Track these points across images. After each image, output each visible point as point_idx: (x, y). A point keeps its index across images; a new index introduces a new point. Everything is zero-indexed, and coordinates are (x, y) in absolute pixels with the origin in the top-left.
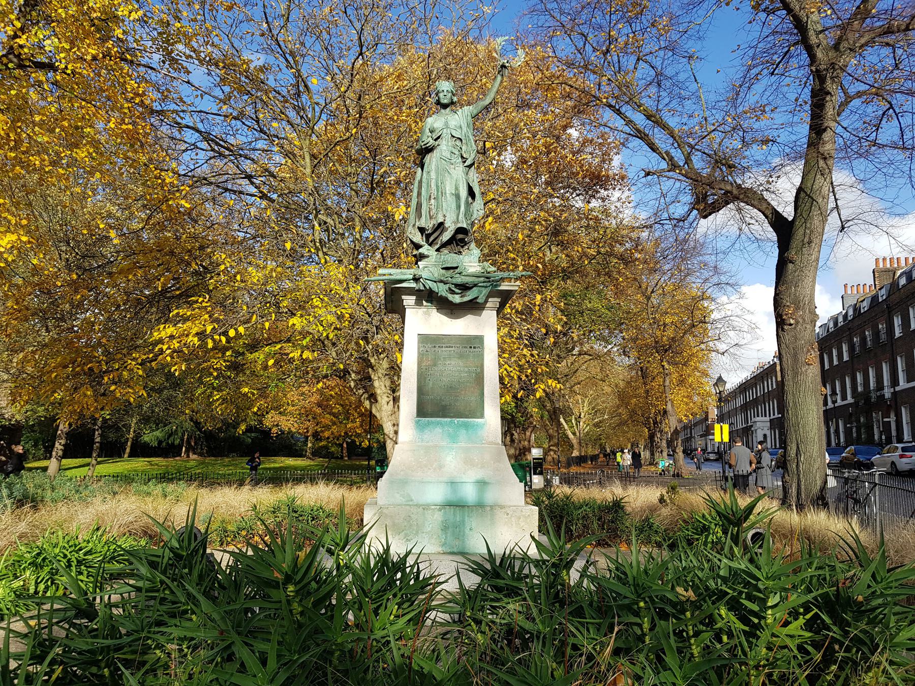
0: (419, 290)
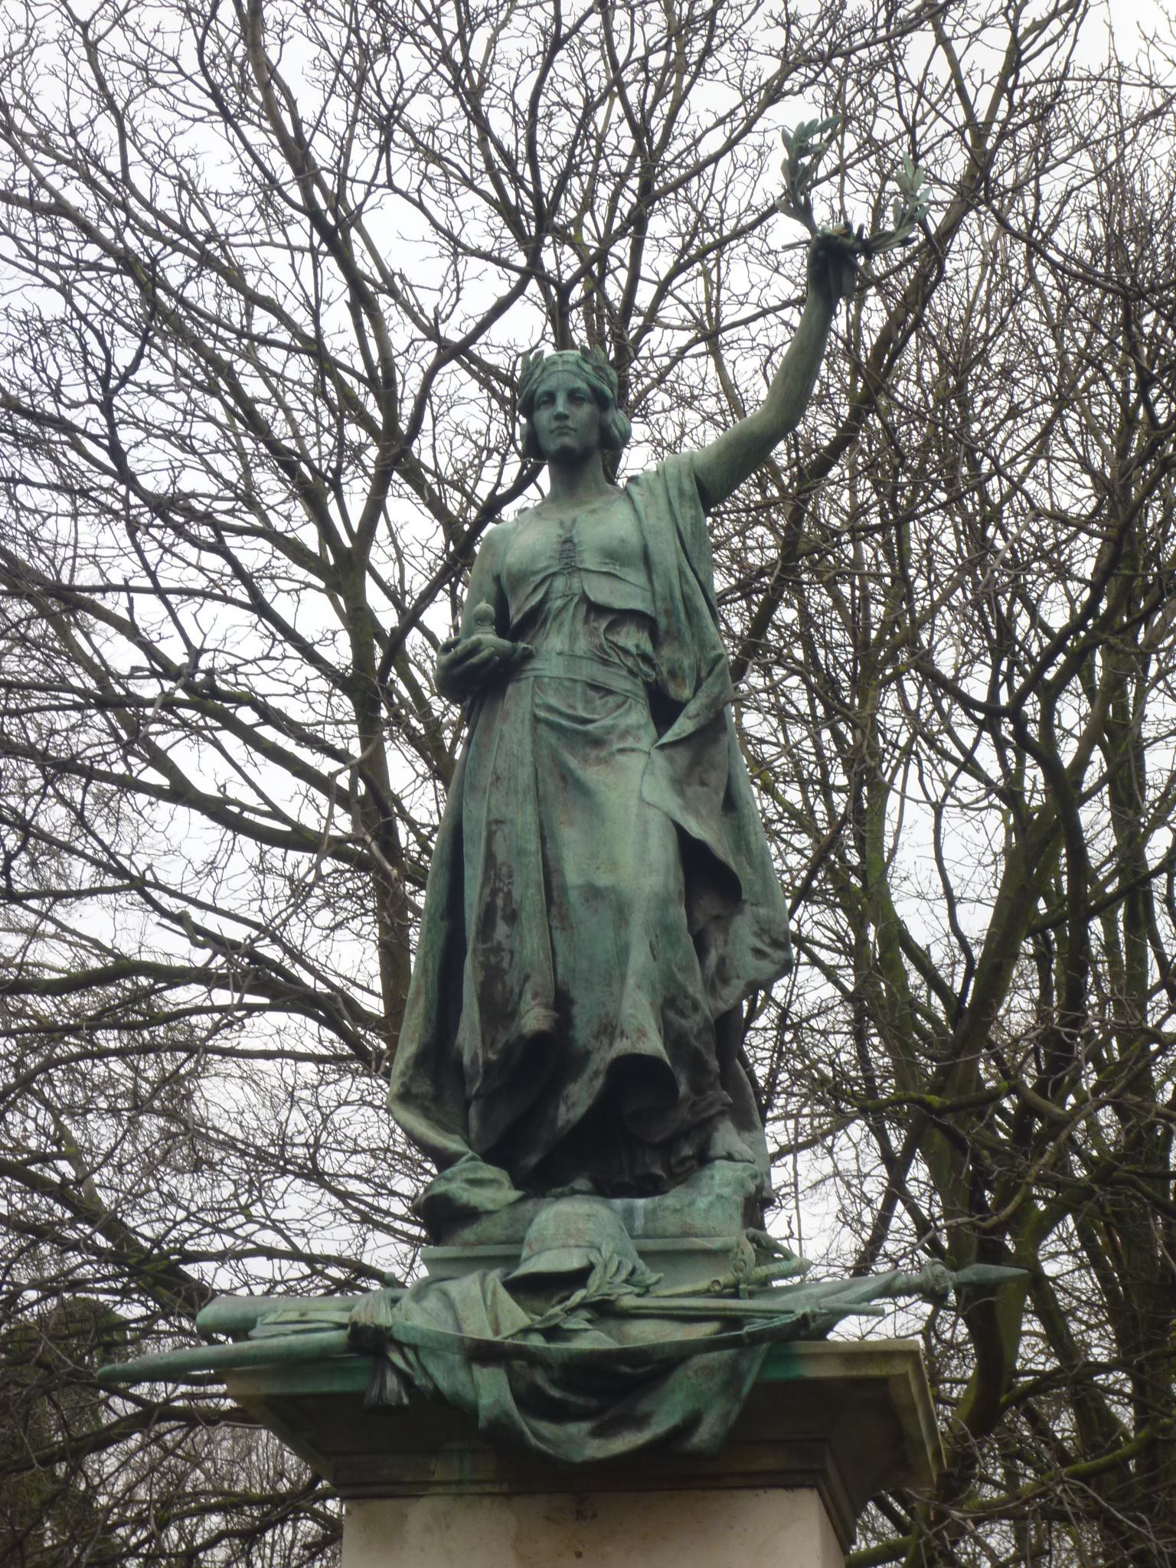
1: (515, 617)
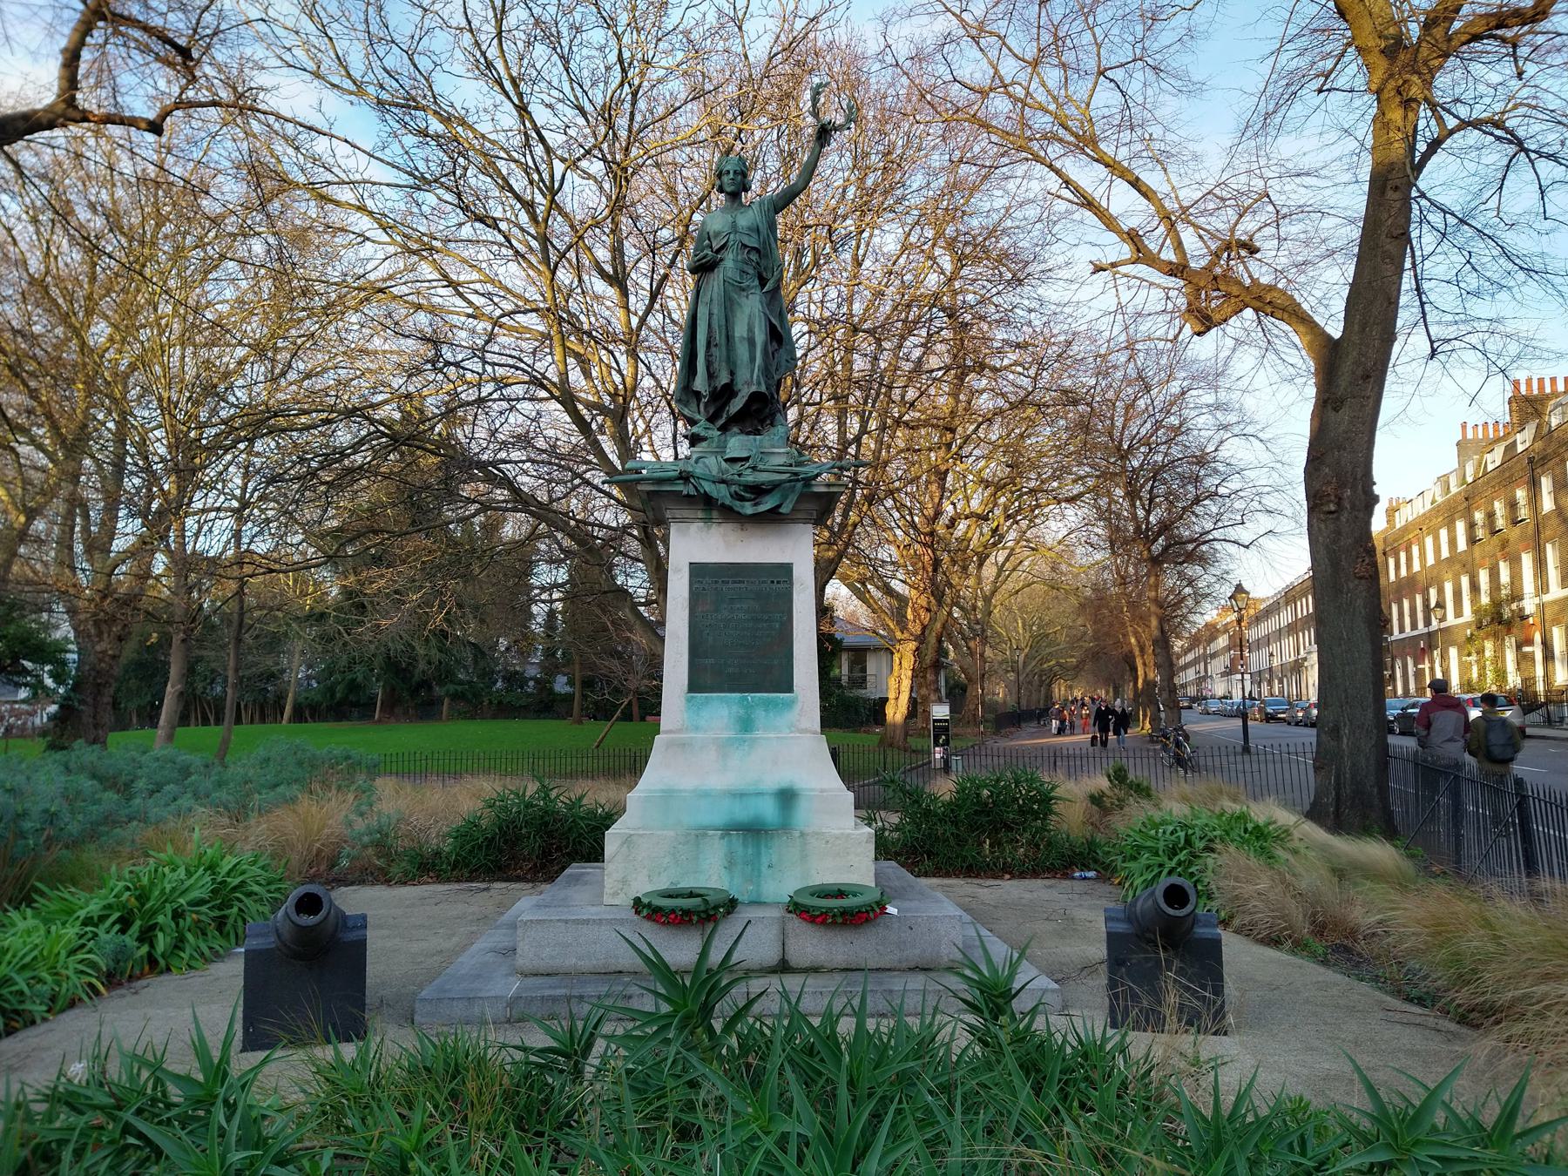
0: (688, 496)
1: (716, 246)
